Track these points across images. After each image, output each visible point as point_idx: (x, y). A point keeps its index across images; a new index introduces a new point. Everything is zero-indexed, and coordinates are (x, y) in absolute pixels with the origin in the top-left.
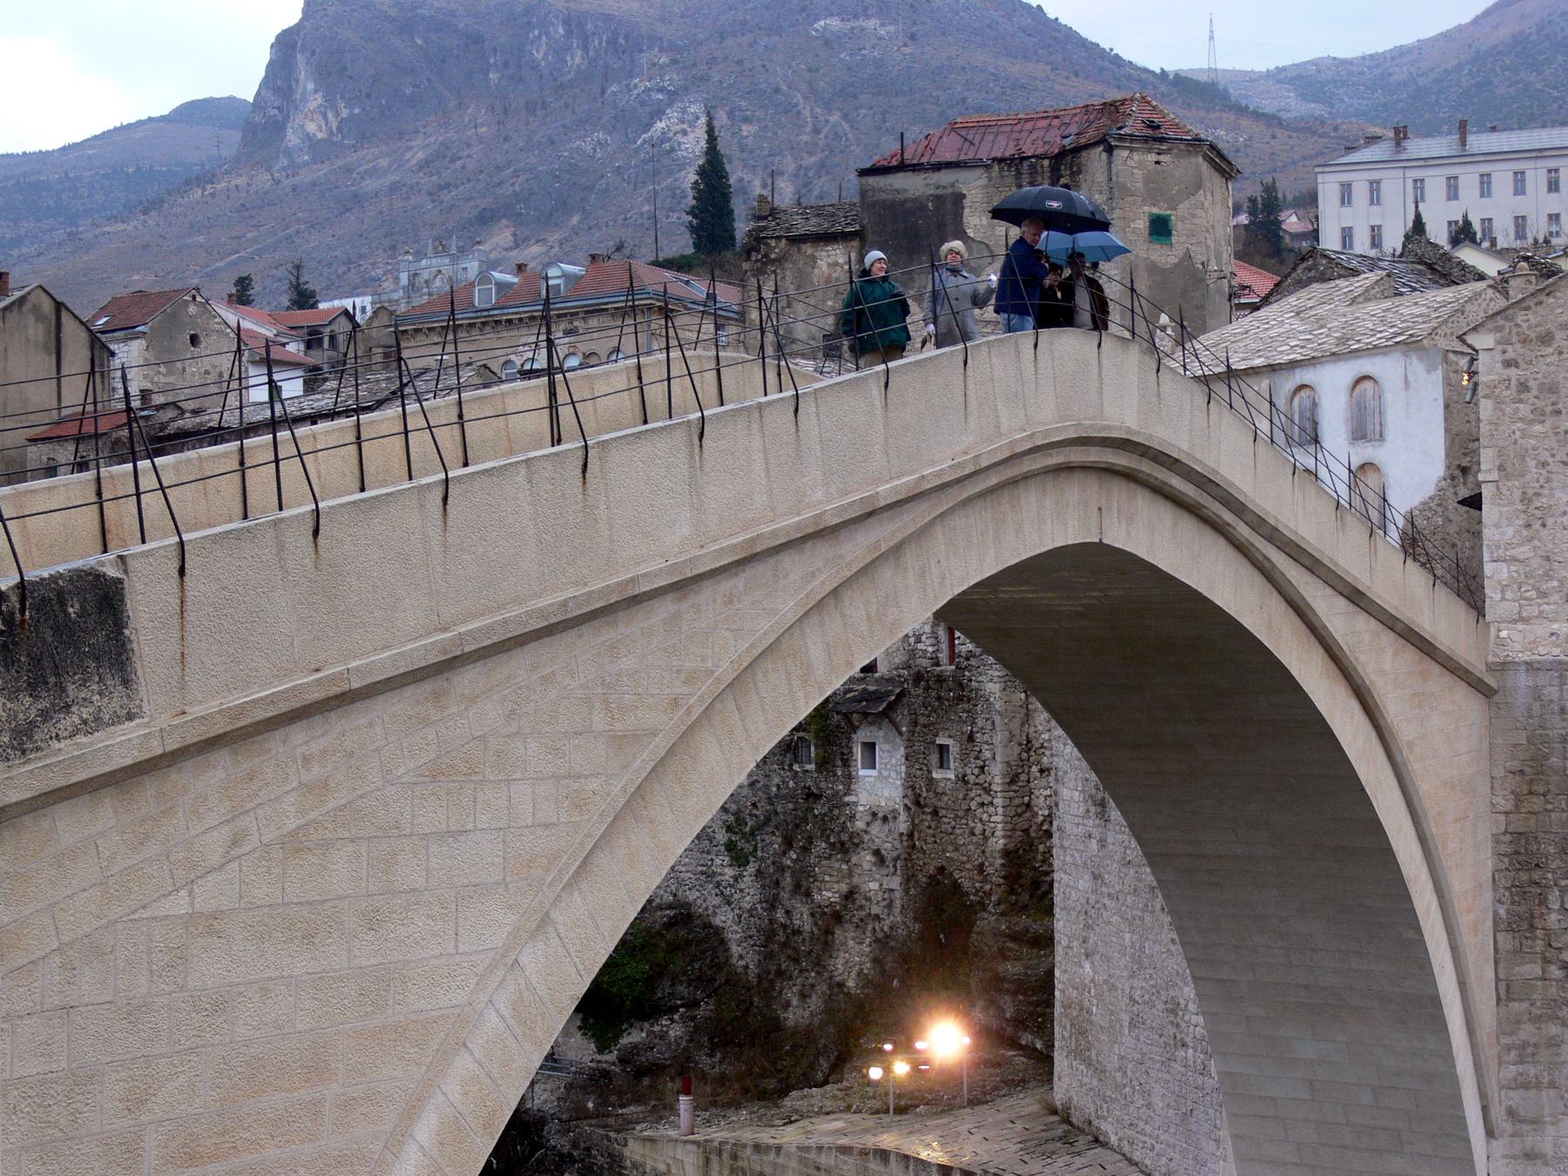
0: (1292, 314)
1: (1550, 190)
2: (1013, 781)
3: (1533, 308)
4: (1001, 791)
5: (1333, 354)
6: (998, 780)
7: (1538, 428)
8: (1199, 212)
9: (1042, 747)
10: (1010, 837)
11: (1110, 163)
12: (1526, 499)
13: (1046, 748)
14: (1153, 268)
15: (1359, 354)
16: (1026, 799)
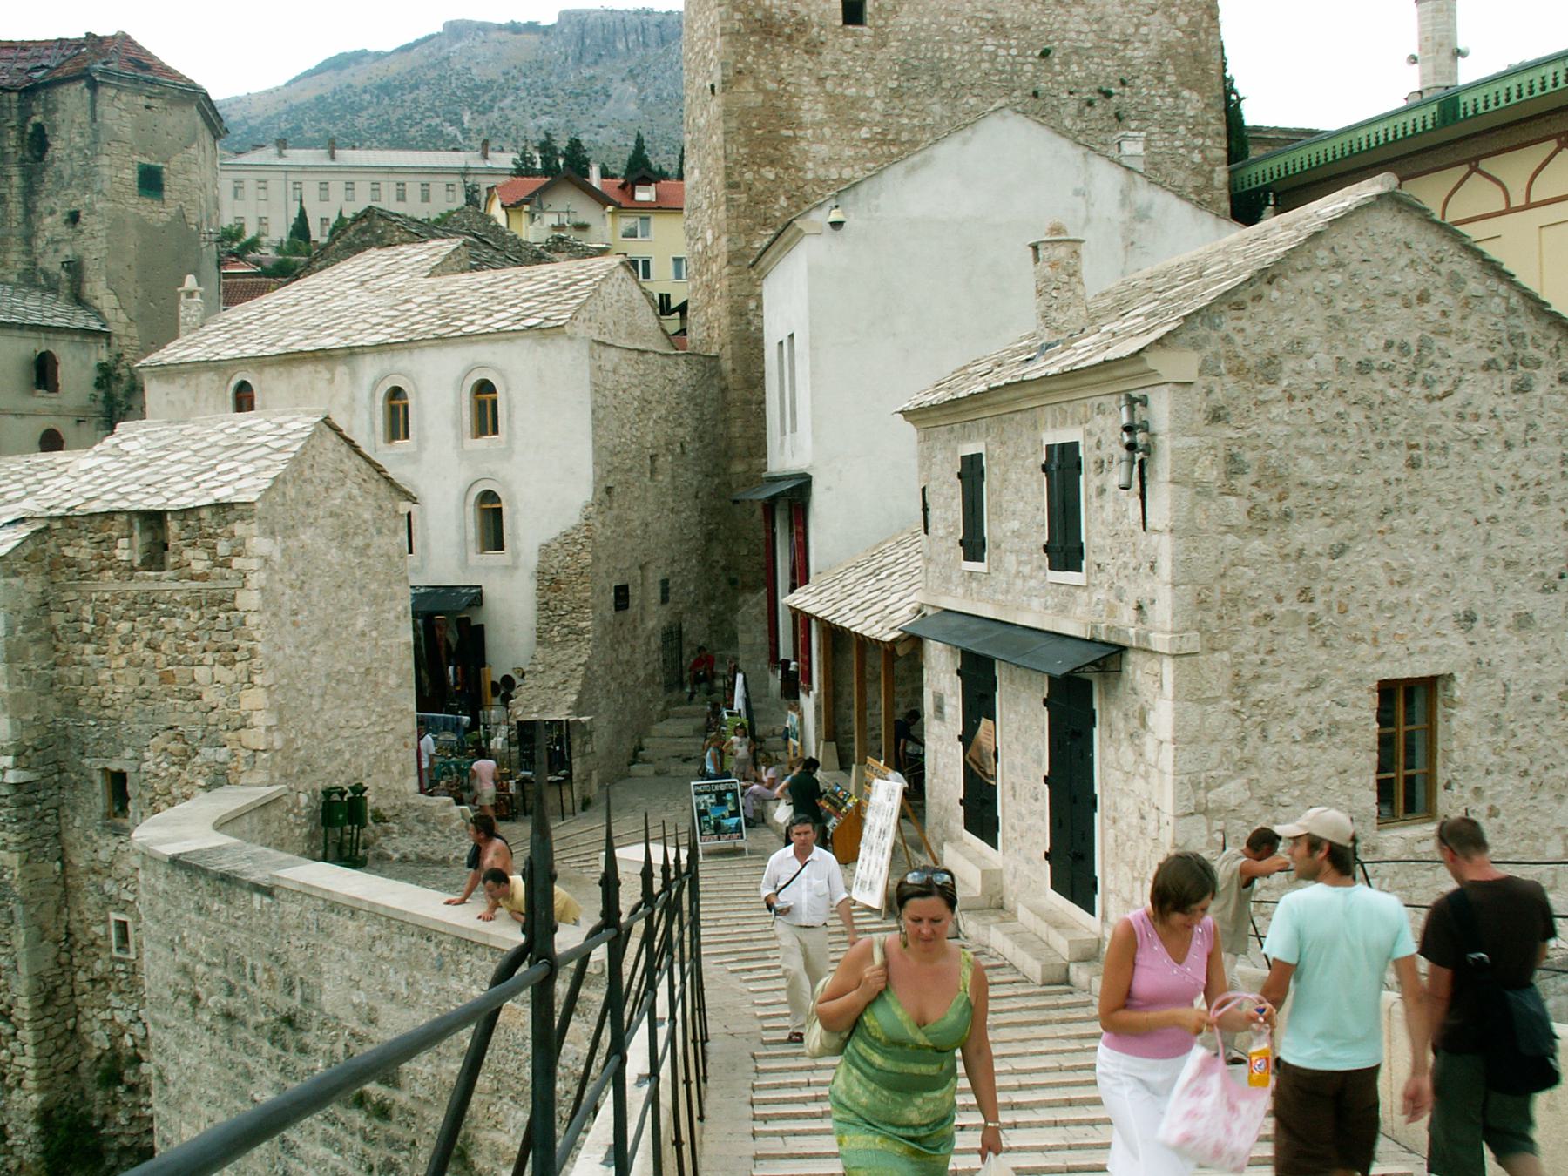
0: (353, 284)
1: (398, 200)
2: (48, 1001)
3: (1249, 304)
4: (31, 1021)
5: (439, 338)
6: (23, 1002)
7: (1257, 545)
8: (194, 168)
9: (93, 944)
10: (49, 1088)
11: (93, 103)
12: (1239, 686)
13: (100, 947)
14: (143, 226)
15: (474, 338)
16: (70, 1023)
